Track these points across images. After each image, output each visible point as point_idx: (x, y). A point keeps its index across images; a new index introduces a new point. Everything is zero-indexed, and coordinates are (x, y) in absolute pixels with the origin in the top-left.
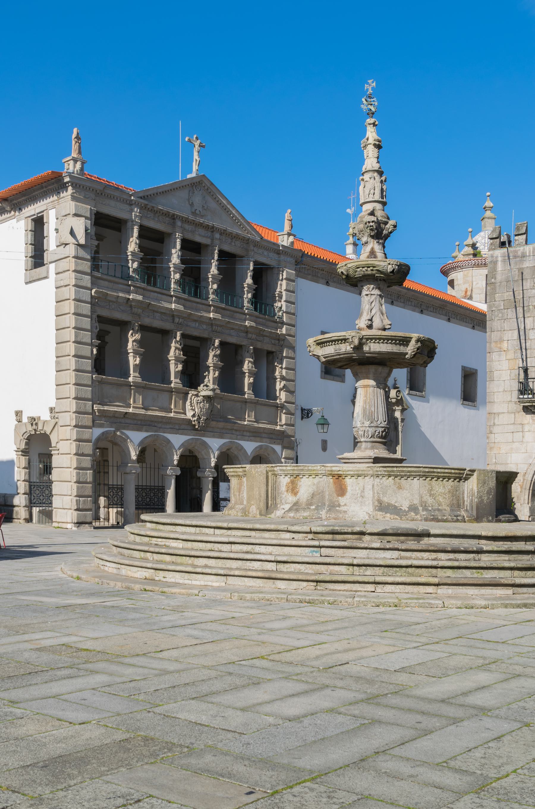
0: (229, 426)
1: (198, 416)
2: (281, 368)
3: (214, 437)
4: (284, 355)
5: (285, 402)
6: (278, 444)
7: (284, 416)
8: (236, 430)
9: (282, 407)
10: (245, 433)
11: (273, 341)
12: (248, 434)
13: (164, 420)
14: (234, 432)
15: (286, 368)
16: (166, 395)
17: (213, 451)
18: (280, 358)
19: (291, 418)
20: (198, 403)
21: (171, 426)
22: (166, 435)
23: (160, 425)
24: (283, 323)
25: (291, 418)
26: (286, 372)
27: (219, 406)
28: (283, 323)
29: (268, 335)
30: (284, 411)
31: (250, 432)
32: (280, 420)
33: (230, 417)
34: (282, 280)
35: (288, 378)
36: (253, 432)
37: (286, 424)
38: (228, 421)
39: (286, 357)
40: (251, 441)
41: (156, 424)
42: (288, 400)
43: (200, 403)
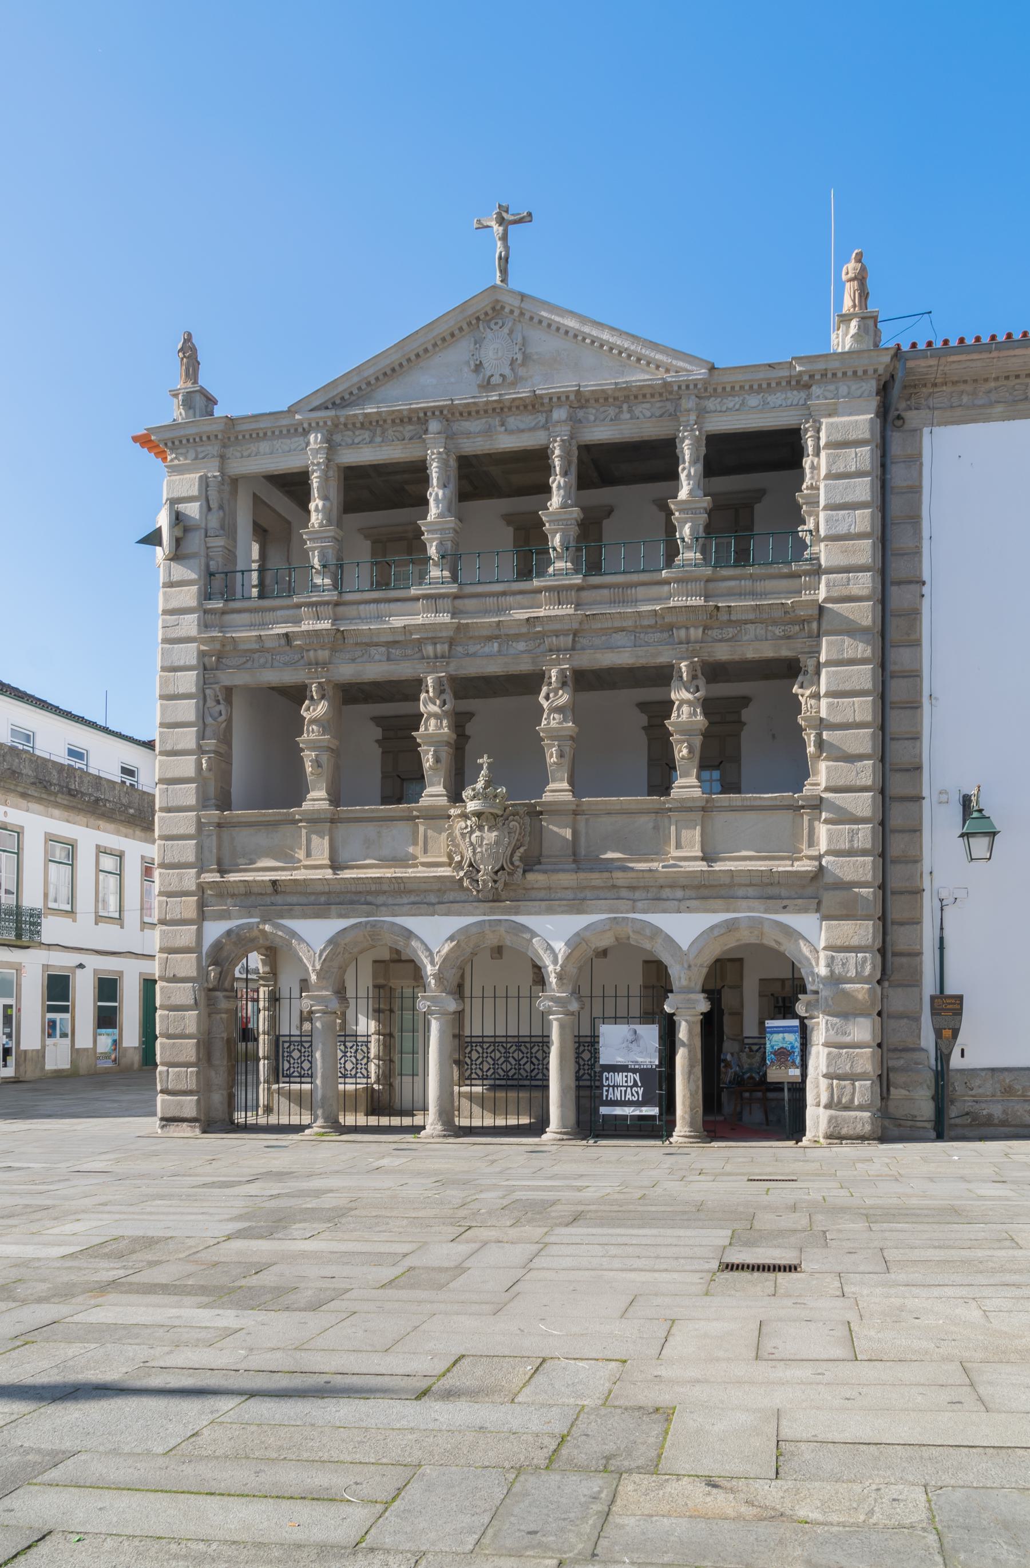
0: (596, 878)
1: (471, 865)
2: (816, 696)
3: (550, 911)
4: (823, 658)
5: (828, 789)
6: (805, 910)
7: (822, 831)
8: (632, 888)
9: (817, 805)
10: (666, 893)
11: (778, 631)
12: (679, 894)
13: (385, 887)
14: (624, 893)
15: (828, 695)
16: (404, 827)
17: (549, 948)
18: (811, 669)
19: (853, 834)
20: (462, 834)
21: (413, 899)
22: (400, 920)
23: (381, 899)
24: (818, 571)
25: (853, 834)
26: (830, 706)
27: (568, 833)
28: (818, 571)
29: (751, 616)
30: (824, 815)
31: (684, 887)
32: (811, 843)
33: (610, 855)
34: (817, 454)
35: (838, 719)
36: (698, 887)
37: (828, 853)
38: (608, 866)
39: (829, 663)
40: (689, 910)
41: (369, 898)
42: (841, 783)
43: (472, 832)
